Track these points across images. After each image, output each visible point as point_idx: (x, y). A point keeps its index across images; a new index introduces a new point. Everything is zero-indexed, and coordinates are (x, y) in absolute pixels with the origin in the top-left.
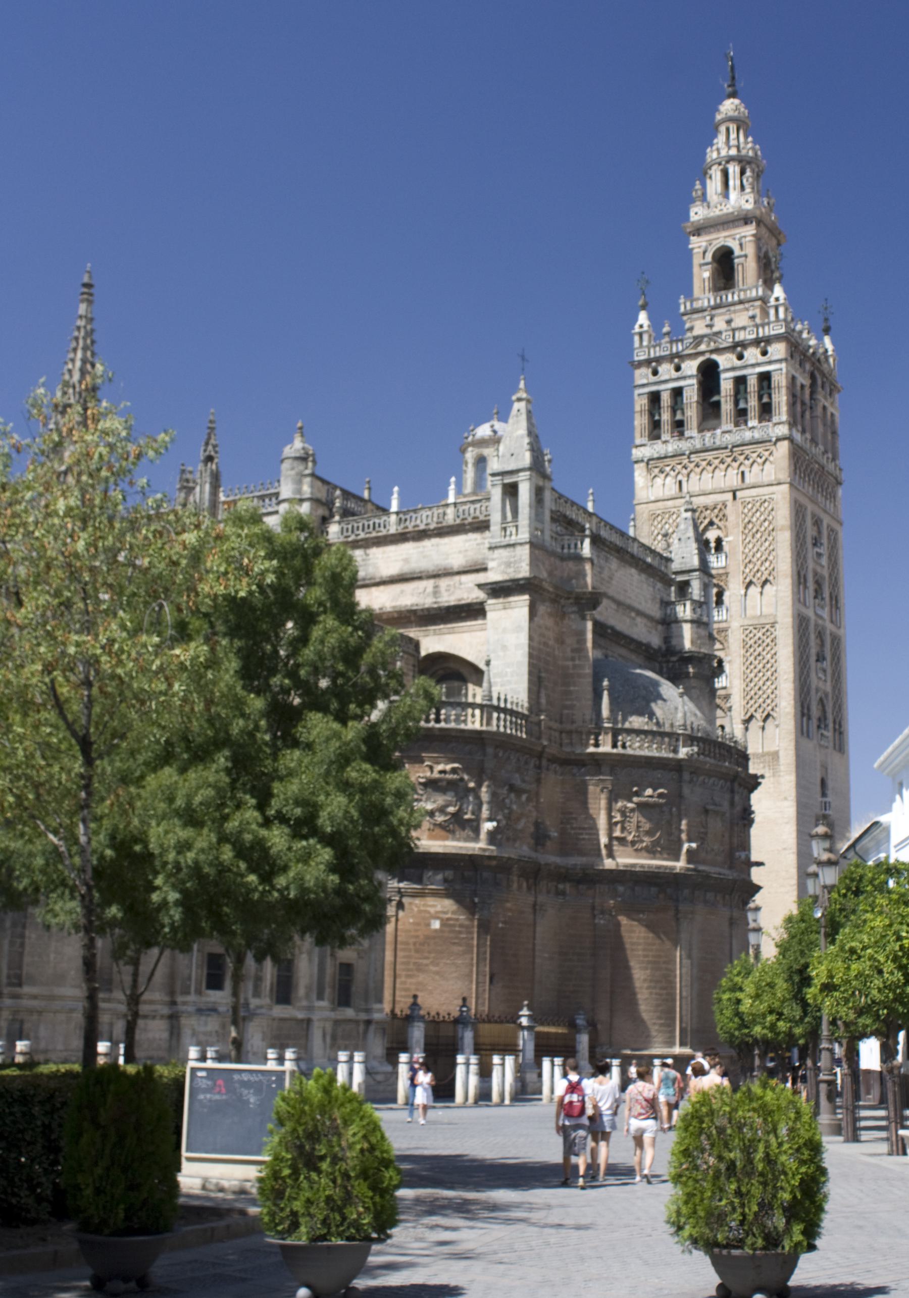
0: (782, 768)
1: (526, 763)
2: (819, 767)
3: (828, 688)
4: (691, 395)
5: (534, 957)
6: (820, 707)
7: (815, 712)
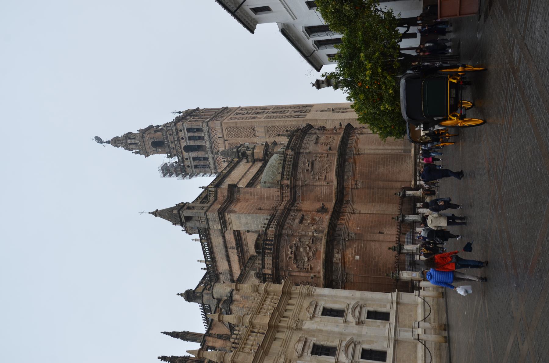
1: (292, 216)
3: (290, 110)
4: (193, 154)
5: (373, 214)
7: (299, 113)
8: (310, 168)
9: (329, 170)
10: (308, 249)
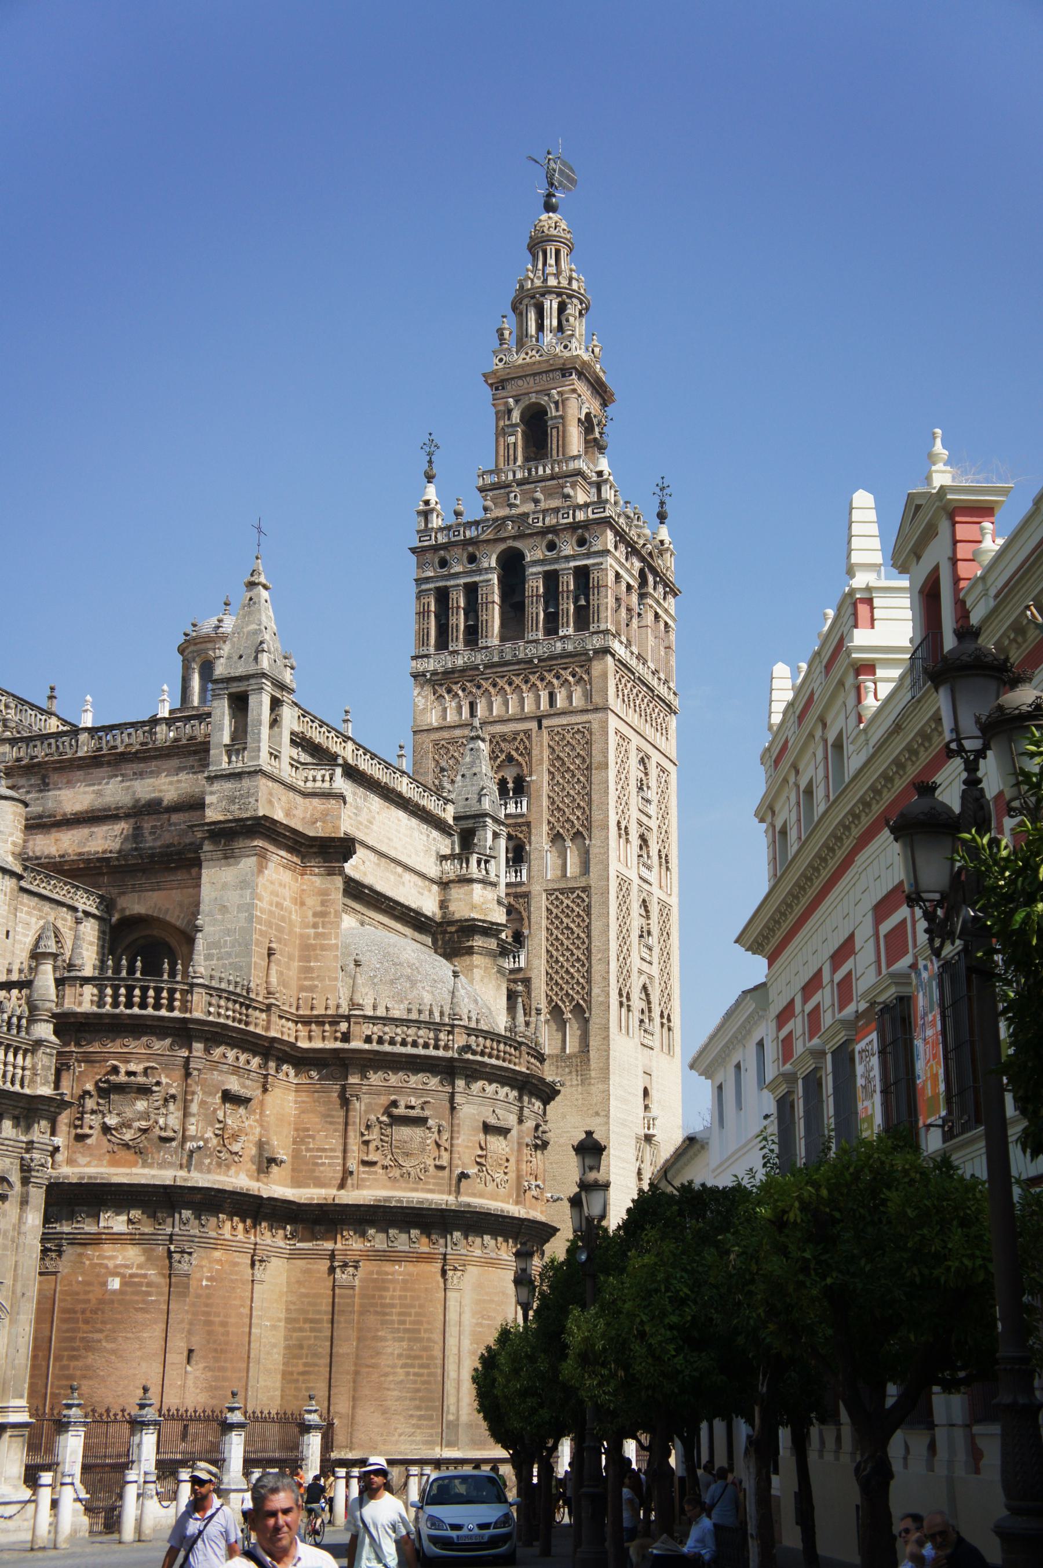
0: (593, 1074)
2: (641, 1074)
3: (655, 970)
6: (643, 996)
8: (401, 1111)
9: (396, 1173)
10: (143, 1124)
